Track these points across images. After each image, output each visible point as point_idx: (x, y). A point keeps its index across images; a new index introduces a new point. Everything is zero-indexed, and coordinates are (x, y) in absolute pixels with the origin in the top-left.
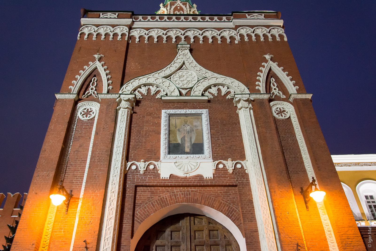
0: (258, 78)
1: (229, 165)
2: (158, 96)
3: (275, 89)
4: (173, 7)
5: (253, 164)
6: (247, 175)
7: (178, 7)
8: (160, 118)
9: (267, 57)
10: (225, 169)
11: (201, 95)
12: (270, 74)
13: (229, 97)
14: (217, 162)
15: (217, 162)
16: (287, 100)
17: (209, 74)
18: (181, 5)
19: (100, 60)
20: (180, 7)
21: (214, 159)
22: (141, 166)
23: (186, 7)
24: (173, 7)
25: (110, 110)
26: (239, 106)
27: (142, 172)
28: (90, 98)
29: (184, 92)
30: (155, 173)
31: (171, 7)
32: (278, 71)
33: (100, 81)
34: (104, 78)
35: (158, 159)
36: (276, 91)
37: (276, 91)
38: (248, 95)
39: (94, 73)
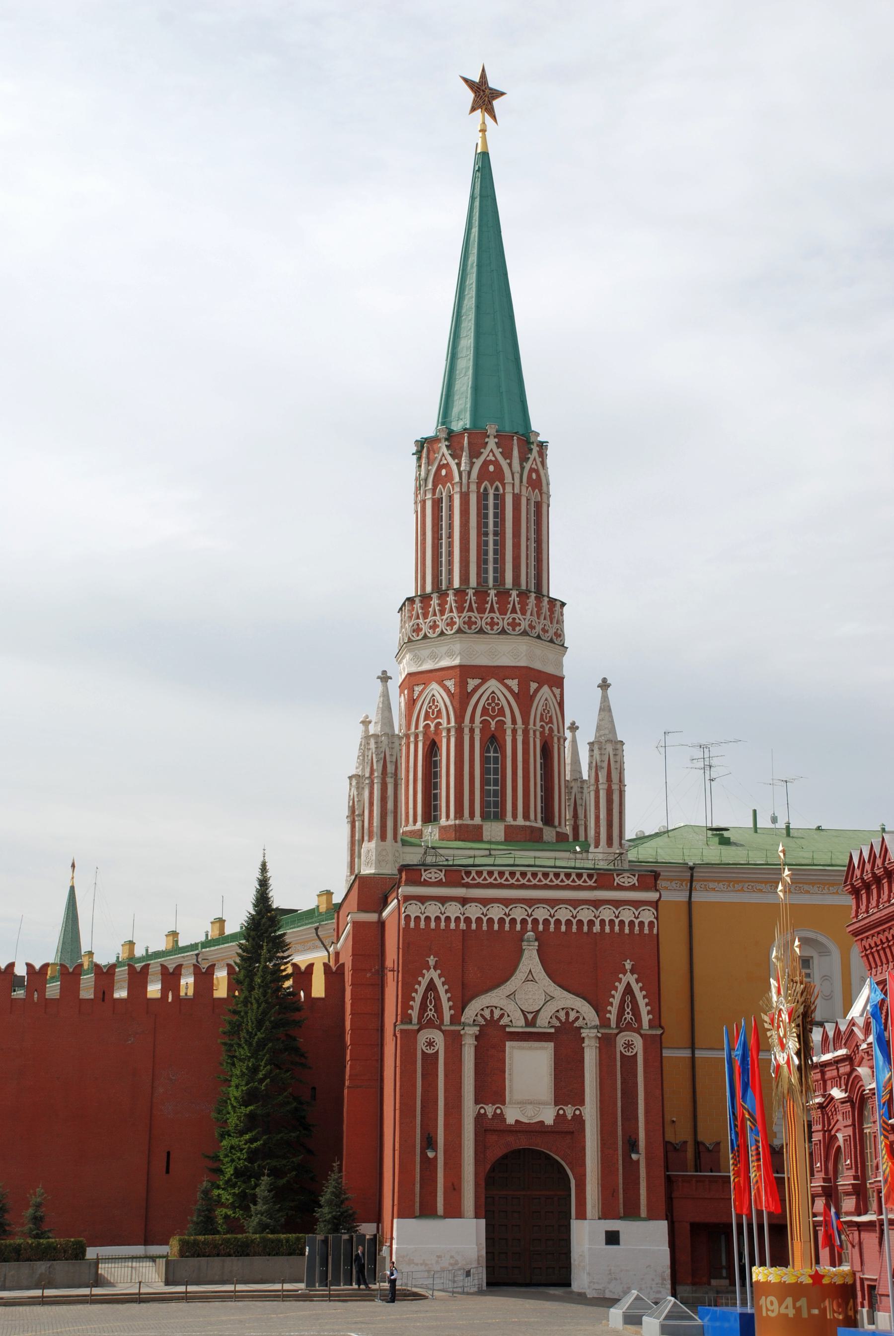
0: (611, 1000)
1: (569, 1111)
2: (502, 1023)
3: (628, 1013)
4: (478, 463)
5: (590, 1111)
6: (584, 1121)
7: (491, 462)
8: (504, 1051)
9: (628, 965)
10: (564, 1115)
11: (547, 1025)
12: (629, 990)
13: (576, 1024)
14: (558, 1108)
15: (558, 1108)
16: (638, 1031)
17: (558, 992)
18: (497, 452)
19: (435, 968)
20: (496, 463)
21: (556, 1104)
22: (490, 1110)
23: (510, 465)
24: (478, 463)
25: (454, 1041)
26: (586, 1041)
27: (490, 1116)
28: (430, 1024)
29: (530, 1017)
30: (501, 1117)
31: (472, 464)
32: (636, 987)
33: (437, 998)
34: (444, 997)
35: (504, 1103)
36: (628, 1016)
37: (628, 1016)
38: (596, 1031)
39: (431, 986)
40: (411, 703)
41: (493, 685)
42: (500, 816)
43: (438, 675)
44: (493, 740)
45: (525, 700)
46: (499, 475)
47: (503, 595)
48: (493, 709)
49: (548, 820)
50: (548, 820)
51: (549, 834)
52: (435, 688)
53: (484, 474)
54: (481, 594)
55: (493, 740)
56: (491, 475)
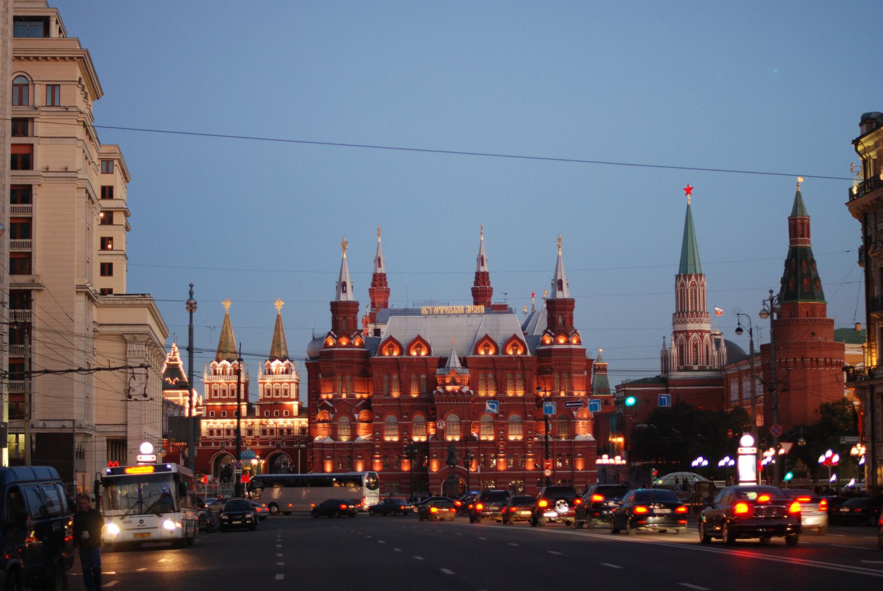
40: (676, 338)
41: (695, 334)
42: (697, 364)
43: (683, 332)
44: (696, 346)
45: (702, 337)
46: (695, 285)
47: (697, 313)
48: (695, 340)
49: (708, 364)
50: (708, 364)
51: (708, 368)
52: (681, 335)
53: (692, 285)
54: (692, 313)
55: (696, 346)
56: (693, 285)
